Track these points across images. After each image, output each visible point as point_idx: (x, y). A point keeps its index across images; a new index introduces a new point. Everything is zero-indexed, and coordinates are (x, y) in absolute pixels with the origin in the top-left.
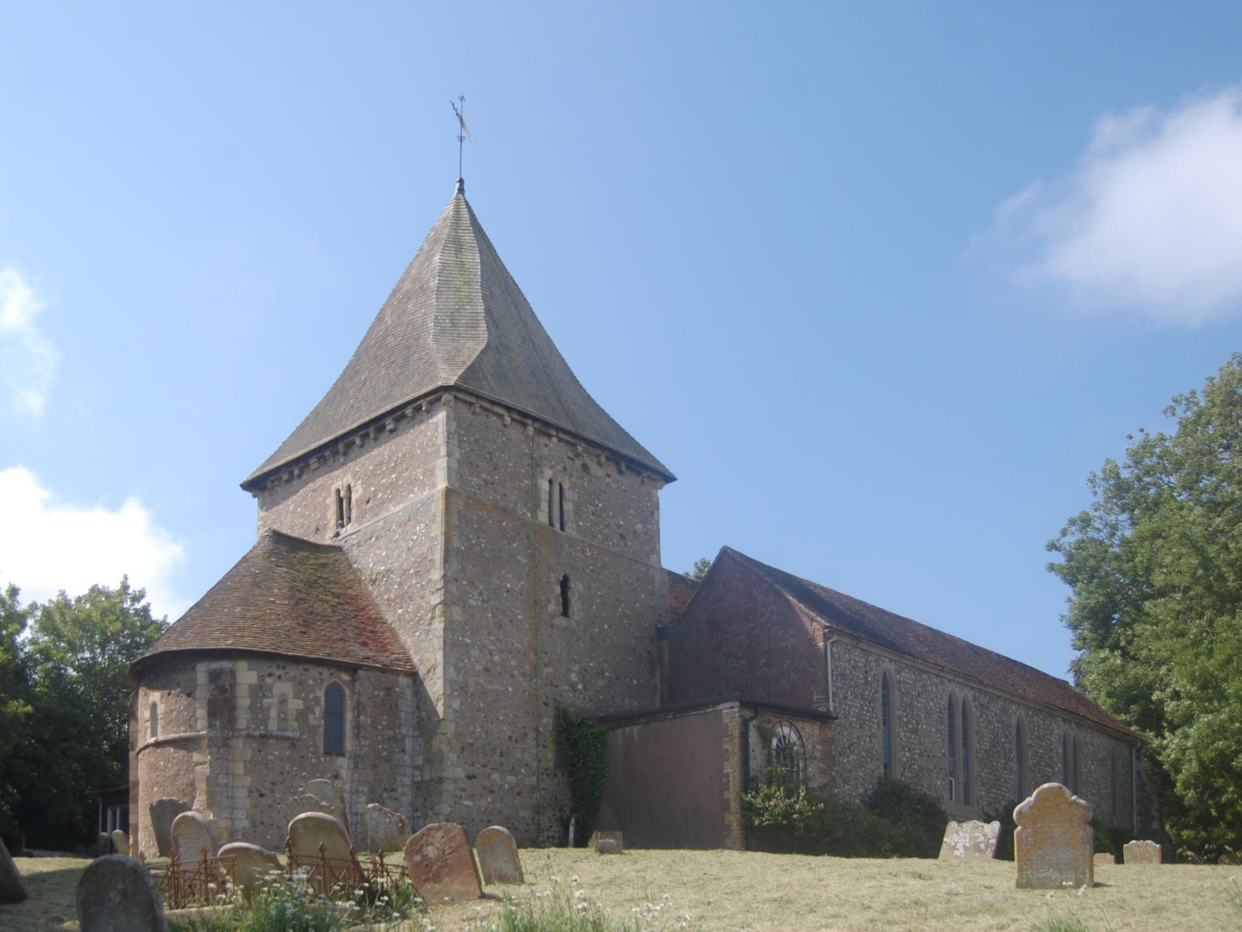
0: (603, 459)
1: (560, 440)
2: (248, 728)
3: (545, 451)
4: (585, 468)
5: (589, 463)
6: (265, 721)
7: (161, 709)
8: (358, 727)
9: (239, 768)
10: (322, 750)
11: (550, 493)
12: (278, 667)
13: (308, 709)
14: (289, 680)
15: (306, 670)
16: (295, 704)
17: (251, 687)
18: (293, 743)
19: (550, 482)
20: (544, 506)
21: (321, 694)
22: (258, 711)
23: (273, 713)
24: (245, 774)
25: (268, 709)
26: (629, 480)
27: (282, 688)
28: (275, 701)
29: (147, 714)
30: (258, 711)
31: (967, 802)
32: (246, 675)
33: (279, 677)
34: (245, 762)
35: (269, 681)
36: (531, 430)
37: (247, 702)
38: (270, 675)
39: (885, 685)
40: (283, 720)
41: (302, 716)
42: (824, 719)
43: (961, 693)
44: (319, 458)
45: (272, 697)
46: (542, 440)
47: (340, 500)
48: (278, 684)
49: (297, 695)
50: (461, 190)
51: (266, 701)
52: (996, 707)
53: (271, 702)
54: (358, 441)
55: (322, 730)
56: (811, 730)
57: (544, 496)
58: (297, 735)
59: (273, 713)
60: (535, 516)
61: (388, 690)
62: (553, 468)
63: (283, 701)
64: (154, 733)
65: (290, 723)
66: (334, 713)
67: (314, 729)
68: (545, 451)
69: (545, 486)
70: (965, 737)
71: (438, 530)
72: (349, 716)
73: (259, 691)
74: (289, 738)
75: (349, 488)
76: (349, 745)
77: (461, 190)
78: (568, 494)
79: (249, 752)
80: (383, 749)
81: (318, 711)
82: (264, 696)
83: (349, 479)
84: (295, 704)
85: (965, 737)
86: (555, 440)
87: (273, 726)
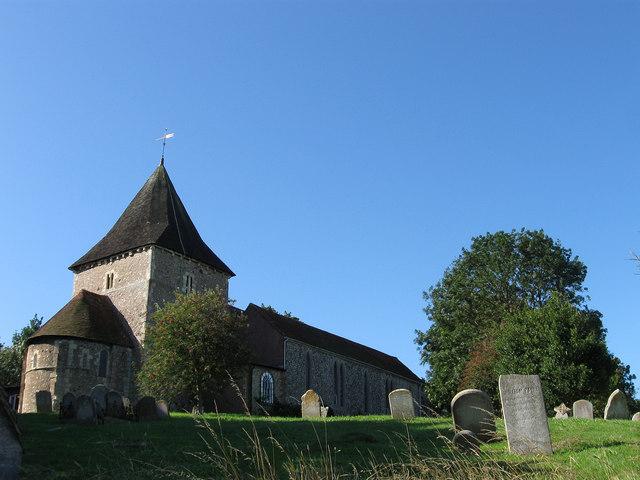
4: (201, 271)
7: (39, 357)
8: (111, 366)
9: (67, 380)
13: (95, 359)
16: (90, 357)
18: (88, 371)
22: (76, 359)
23: (82, 360)
26: (217, 275)
27: (85, 351)
29: (33, 358)
30: (76, 359)
31: (342, 405)
32: (73, 345)
37: (72, 355)
39: (308, 359)
41: (92, 361)
42: (283, 370)
43: (340, 361)
47: (109, 278)
50: (162, 163)
52: (355, 368)
56: (277, 374)
57: (185, 282)
59: (82, 360)
62: (189, 269)
63: (86, 356)
64: (35, 364)
66: (103, 361)
67: (95, 366)
69: (185, 278)
70: (342, 379)
71: (145, 295)
73: (77, 352)
77: (162, 163)
81: (98, 360)
83: (113, 271)
85: (342, 379)
87: (81, 364)
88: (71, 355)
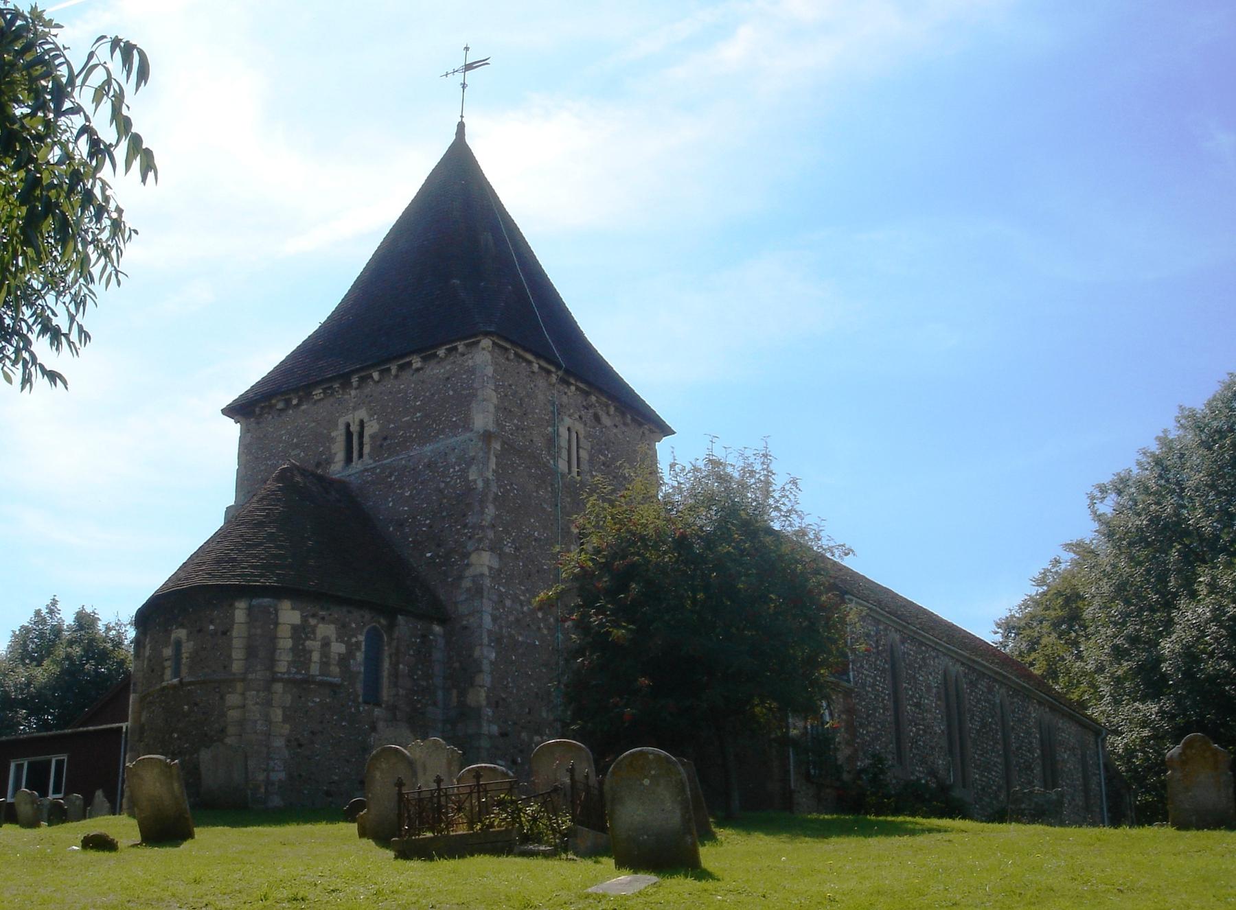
0: (612, 410)
1: (578, 388)
2: (288, 672)
3: (565, 399)
4: (597, 418)
5: (600, 413)
6: (306, 663)
8: (395, 674)
10: (360, 699)
11: (569, 441)
12: (322, 608)
13: (350, 654)
14: (332, 622)
15: (349, 612)
16: (338, 648)
17: (295, 628)
19: (569, 429)
20: (564, 454)
21: (361, 638)
22: (300, 655)
23: (316, 656)
24: (284, 721)
25: (311, 652)
28: (317, 644)
30: (300, 655)
33: (323, 618)
34: (284, 708)
35: (313, 622)
36: (554, 378)
37: (289, 643)
38: (314, 616)
40: (325, 663)
41: (344, 660)
44: (325, 390)
45: (314, 639)
46: (563, 388)
48: (321, 625)
49: (340, 639)
51: (308, 643)
53: (313, 645)
54: (376, 376)
55: (362, 676)
57: (564, 443)
58: (337, 680)
59: (316, 656)
60: (556, 462)
61: (424, 636)
63: (326, 644)
65: (332, 668)
68: (565, 399)
72: (386, 664)
73: (301, 633)
74: (331, 685)
75: (362, 423)
76: (386, 694)
78: (585, 444)
79: (290, 697)
80: (419, 701)
81: (360, 656)
82: (308, 638)
83: (362, 414)
84: (338, 648)
86: (573, 388)
87: (315, 669)
88: (285, 643)
